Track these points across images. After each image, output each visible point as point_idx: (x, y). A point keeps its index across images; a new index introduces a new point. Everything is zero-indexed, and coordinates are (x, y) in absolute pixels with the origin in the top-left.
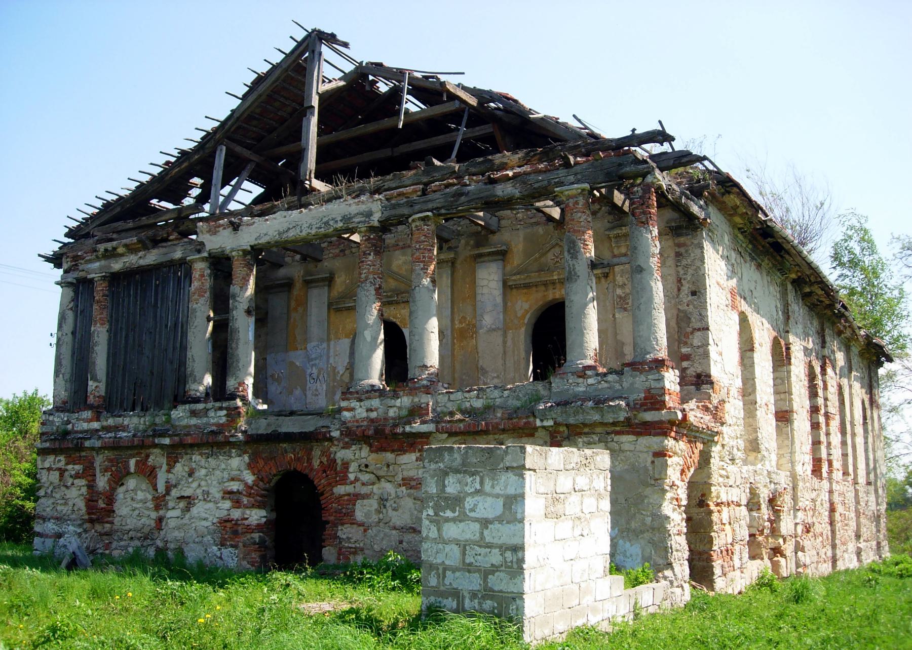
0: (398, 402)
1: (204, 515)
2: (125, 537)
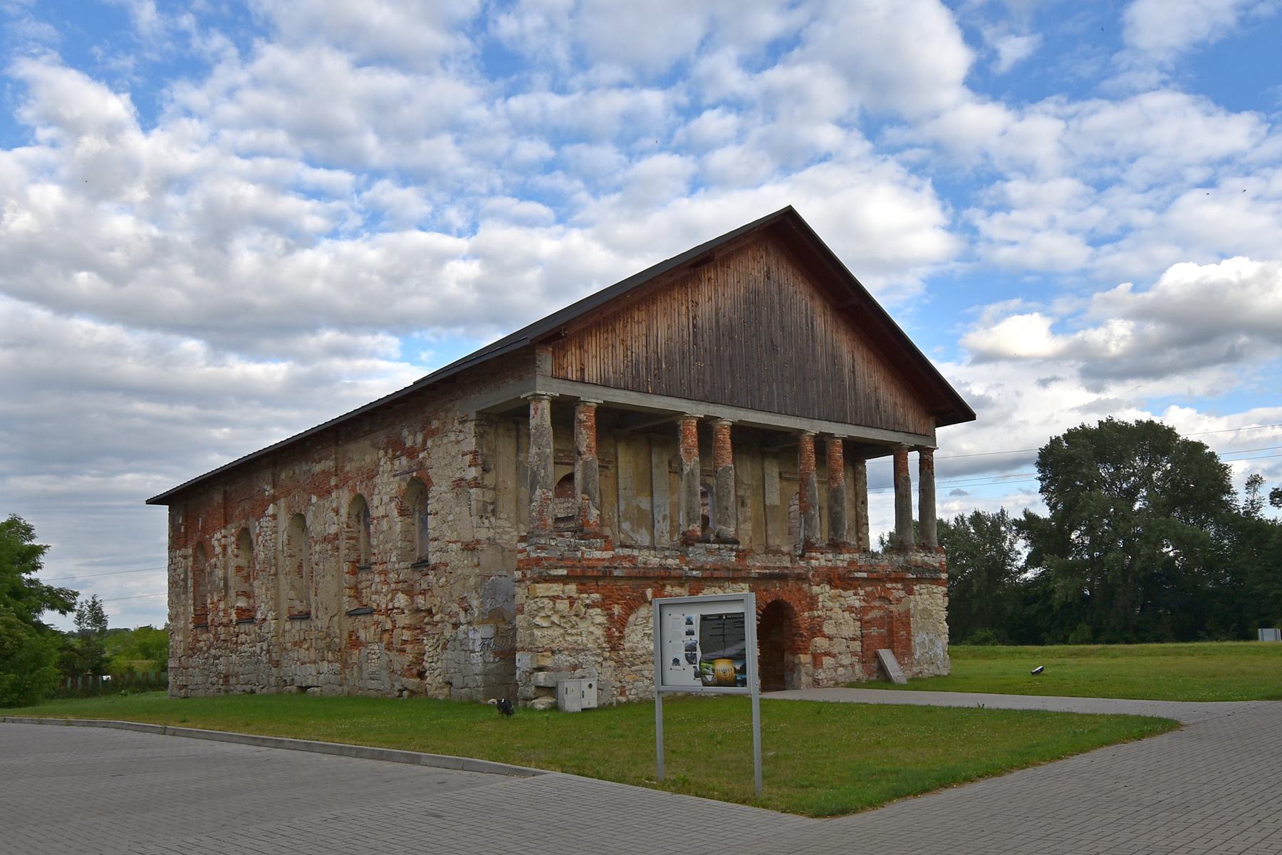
0: (841, 557)
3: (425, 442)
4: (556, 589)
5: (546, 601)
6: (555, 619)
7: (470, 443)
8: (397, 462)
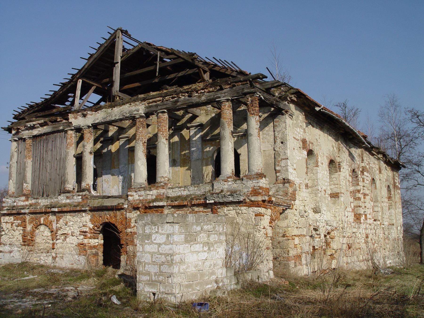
0: (151, 193)
1: (72, 242)
4: (7, 218)
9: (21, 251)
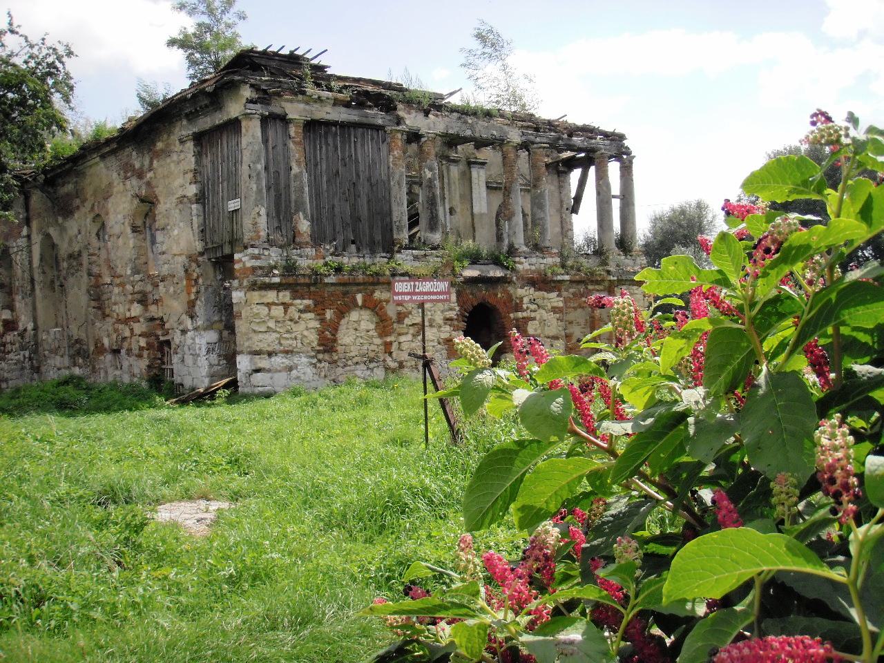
2: (350, 363)
3: (151, 163)
4: (271, 296)
5: (263, 307)
6: (272, 324)
7: (189, 160)
8: (128, 183)
9: (318, 365)
